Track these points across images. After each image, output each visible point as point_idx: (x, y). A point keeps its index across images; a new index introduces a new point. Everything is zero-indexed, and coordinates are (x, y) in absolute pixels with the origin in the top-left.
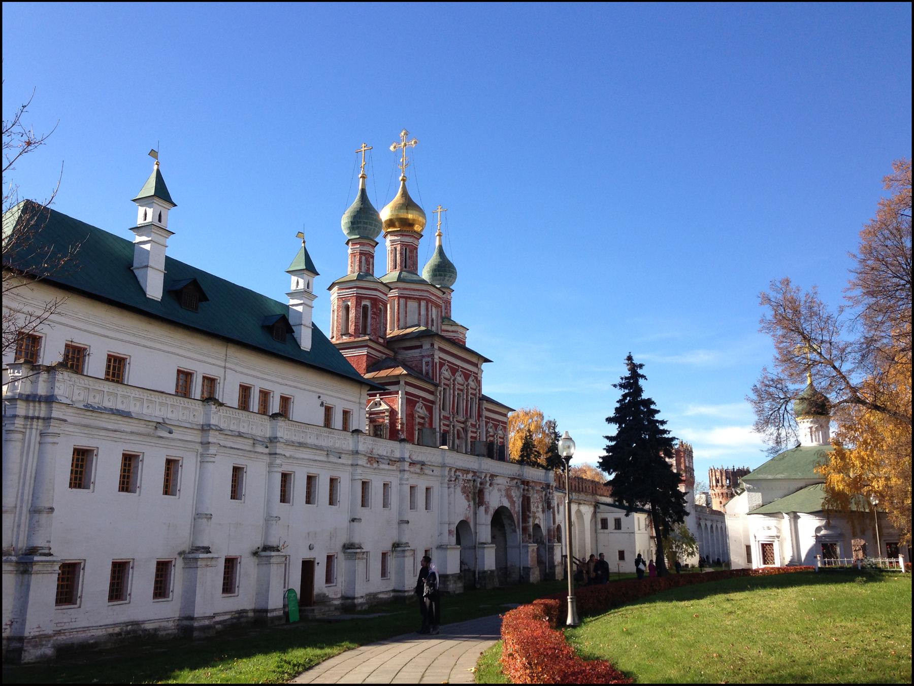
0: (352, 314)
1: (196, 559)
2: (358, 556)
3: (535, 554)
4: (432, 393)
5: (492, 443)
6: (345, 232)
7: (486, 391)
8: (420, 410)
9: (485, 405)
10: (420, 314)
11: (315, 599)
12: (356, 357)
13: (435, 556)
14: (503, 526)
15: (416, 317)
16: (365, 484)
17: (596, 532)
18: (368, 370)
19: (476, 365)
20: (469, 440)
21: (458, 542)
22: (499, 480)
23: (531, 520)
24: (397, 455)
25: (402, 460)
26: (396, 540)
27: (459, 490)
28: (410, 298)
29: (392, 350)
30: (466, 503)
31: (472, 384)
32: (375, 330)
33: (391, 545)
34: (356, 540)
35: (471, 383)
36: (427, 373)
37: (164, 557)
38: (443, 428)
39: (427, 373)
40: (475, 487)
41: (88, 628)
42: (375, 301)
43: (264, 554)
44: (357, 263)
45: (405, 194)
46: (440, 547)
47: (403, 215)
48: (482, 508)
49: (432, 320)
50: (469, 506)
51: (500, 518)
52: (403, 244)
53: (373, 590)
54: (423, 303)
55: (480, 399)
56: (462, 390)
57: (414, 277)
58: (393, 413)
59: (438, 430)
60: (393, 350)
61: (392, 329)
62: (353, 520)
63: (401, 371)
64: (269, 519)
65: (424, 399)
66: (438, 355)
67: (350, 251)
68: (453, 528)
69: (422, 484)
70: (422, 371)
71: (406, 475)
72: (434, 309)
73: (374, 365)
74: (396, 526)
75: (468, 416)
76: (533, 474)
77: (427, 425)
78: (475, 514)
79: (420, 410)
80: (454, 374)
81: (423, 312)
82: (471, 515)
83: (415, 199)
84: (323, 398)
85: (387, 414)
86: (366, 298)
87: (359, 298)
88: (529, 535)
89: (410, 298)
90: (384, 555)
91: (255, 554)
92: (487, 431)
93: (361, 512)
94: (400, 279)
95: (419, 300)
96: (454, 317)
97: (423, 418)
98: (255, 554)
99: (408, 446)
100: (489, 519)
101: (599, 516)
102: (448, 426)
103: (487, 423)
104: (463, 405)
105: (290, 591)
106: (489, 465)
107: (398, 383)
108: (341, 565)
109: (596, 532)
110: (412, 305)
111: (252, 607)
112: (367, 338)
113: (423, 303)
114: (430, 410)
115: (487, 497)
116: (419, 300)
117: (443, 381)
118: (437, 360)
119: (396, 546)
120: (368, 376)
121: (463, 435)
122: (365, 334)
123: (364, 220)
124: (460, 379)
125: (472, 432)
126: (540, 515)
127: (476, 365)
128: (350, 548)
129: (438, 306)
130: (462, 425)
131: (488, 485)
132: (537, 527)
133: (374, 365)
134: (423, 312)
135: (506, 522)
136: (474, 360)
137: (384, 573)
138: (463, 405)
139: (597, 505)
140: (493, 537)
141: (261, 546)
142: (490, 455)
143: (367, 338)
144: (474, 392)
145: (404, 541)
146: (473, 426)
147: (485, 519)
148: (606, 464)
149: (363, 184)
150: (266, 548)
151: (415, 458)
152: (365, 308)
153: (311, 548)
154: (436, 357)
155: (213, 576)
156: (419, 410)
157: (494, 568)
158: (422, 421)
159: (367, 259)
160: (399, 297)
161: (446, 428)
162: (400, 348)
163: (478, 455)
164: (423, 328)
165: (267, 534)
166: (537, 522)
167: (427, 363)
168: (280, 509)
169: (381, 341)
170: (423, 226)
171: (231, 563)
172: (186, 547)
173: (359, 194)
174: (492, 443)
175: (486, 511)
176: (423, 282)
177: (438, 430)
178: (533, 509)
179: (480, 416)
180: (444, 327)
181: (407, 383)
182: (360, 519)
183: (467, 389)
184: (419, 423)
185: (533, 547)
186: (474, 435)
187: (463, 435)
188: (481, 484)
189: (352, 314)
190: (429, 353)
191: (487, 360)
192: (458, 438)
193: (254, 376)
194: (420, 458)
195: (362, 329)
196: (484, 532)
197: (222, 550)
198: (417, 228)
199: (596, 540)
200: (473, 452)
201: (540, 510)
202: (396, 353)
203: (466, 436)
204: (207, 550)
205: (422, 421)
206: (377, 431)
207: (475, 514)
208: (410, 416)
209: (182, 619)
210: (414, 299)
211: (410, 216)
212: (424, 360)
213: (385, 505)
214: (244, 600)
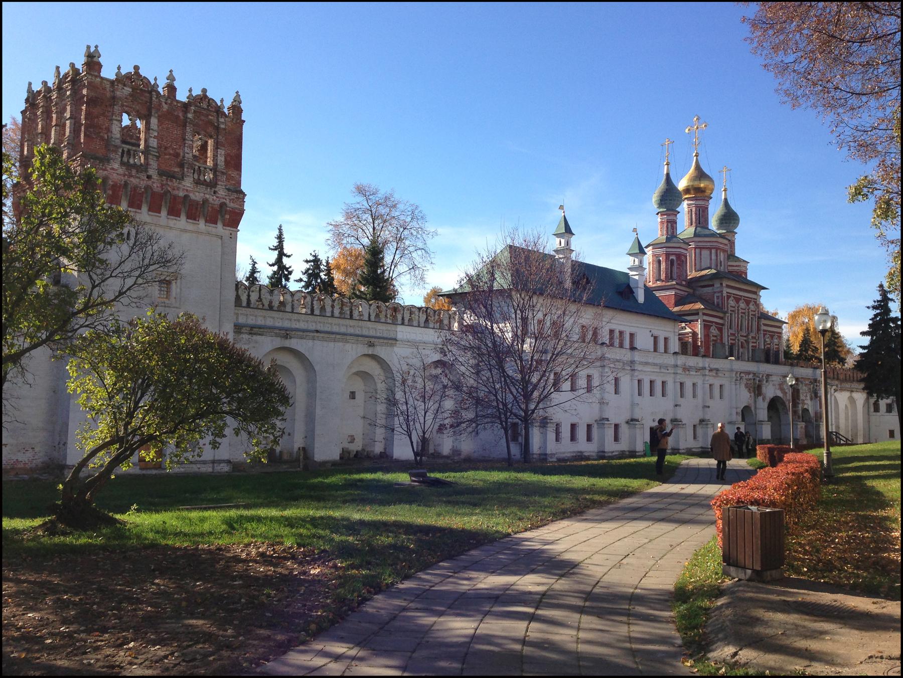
0: (663, 266)
4: (721, 318)
5: (769, 349)
6: (656, 206)
8: (714, 331)
9: (763, 321)
12: (667, 296)
14: (777, 410)
18: (676, 305)
19: (755, 293)
21: (743, 420)
22: (774, 378)
23: (800, 406)
24: (701, 365)
25: (704, 368)
26: (702, 417)
29: (692, 288)
30: (749, 395)
31: (752, 307)
32: (679, 276)
34: (678, 417)
36: (718, 305)
37: (590, 423)
39: (718, 305)
40: (755, 383)
41: (564, 453)
42: (679, 256)
44: (665, 229)
45: (698, 167)
47: (696, 183)
48: (760, 398)
51: (775, 405)
52: (697, 206)
53: (689, 446)
54: (713, 251)
55: (759, 318)
57: (707, 232)
58: (694, 334)
60: (692, 290)
61: (691, 271)
62: (676, 406)
63: (699, 306)
64: (633, 405)
65: (716, 323)
66: (726, 291)
67: (659, 220)
68: (740, 410)
69: (717, 383)
71: (707, 378)
73: (679, 301)
78: (755, 402)
79: (714, 331)
81: (714, 257)
82: (752, 402)
83: (706, 170)
87: (668, 255)
88: (799, 417)
90: (695, 426)
91: (627, 422)
92: (765, 341)
93: (681, 401)
94: (696, 235)
95: (710, 249)
96: (738, 254)
98: (627, 422)
99: (708, 360)
100: (766, 405)
103: (764, 335)
104: (745, 323)
105: (646, 442)
107: (697, 314)
110: (705, 253)
112: (674, 283)
113: (713, 251)
114: (720, 330)
115: (764, 390)
116: (710, 249)
117: (730, 309)
119: (702, 421)
120: (676, 309)
121: (745, 345)
122: (672, 279)
123: (669, 198)
124: (742, 305)
126: (808, 402)
127: (755, 293)
129: (724, 251)
133: (679, 301)
134: (714, 257)
135: (780, 407)
136: (754, 290)
137: (695, 438)
138: (745, 323)
142: (767, 361)
143: (674, 283)
145: (707, 418)
149: (668, 169)
150: (632, 420)
151: (712, 366)
152: (672, 261)
155: (610, 432)
159: (671, 225)
160: (695, 248)
164: (714, 271)
165: (632, 411)
166: (806, 407)
167: (718, 297)
168: (638, 399)
169: (684, 283)
170: (712, 190)
171: (616, 426)
172: (597, 418)
173: (665, 177)
174: (769, 349)
175: (764, 399)
176: (714, 235)
178: (802, 397)
179: (759, 330)
180: (730, 263)
181: (704, 314)
187: (745, 345)
189: (663, 266)
191: (764, 288)
192: (742, 347)
194: (715, 366)
195: (670, 277)
196: (762, 413)
197: (614, 420)
198: (708, 192)
200: (754, 359)
201: (808, 398)
202: (694, 290)
204: (607, 420)
206: (684, 345)
207: (755, 402)
208: (707, 336)
209: (599, 452)
211: (702, 185)
212: (716, 295)
213: (694, 396)
214: (623, 446)
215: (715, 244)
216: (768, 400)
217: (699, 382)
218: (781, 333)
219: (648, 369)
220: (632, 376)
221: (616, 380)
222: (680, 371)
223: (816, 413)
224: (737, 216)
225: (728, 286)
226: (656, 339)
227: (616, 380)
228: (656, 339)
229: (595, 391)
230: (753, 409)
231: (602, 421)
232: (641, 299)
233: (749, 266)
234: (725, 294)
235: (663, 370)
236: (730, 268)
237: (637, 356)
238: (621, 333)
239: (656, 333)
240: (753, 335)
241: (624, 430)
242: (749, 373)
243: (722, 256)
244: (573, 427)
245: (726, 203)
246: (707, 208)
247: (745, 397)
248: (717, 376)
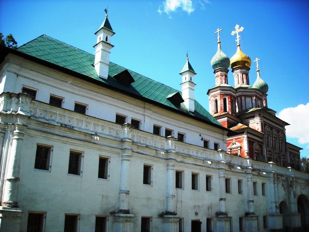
27: (280, 185)
35: (281, 135)
38: (268, 156)
50: (286, 194)
56: (276, 138)
59: (266, 156)
69: (259, 181)
72: (259, 101)
73: (231, 124)
77: (260, 154)
84: (202, 136)
102: (270, 155)
104: (277, 145)
114: (261, 146)
117: (267, 133)
124: (275, 132)
130: (278, 155)
138: (277, 145)
144: (282, 139)
158: (257, 152)
161: (270, 156)
177: (266, 156)
183: (279, 137)
184: (256, 153)
187: (278, 160)
188: (291, 182)
193: (161, 121)
203: (280, 161)
205: (257, 152)
247: (282, 193)
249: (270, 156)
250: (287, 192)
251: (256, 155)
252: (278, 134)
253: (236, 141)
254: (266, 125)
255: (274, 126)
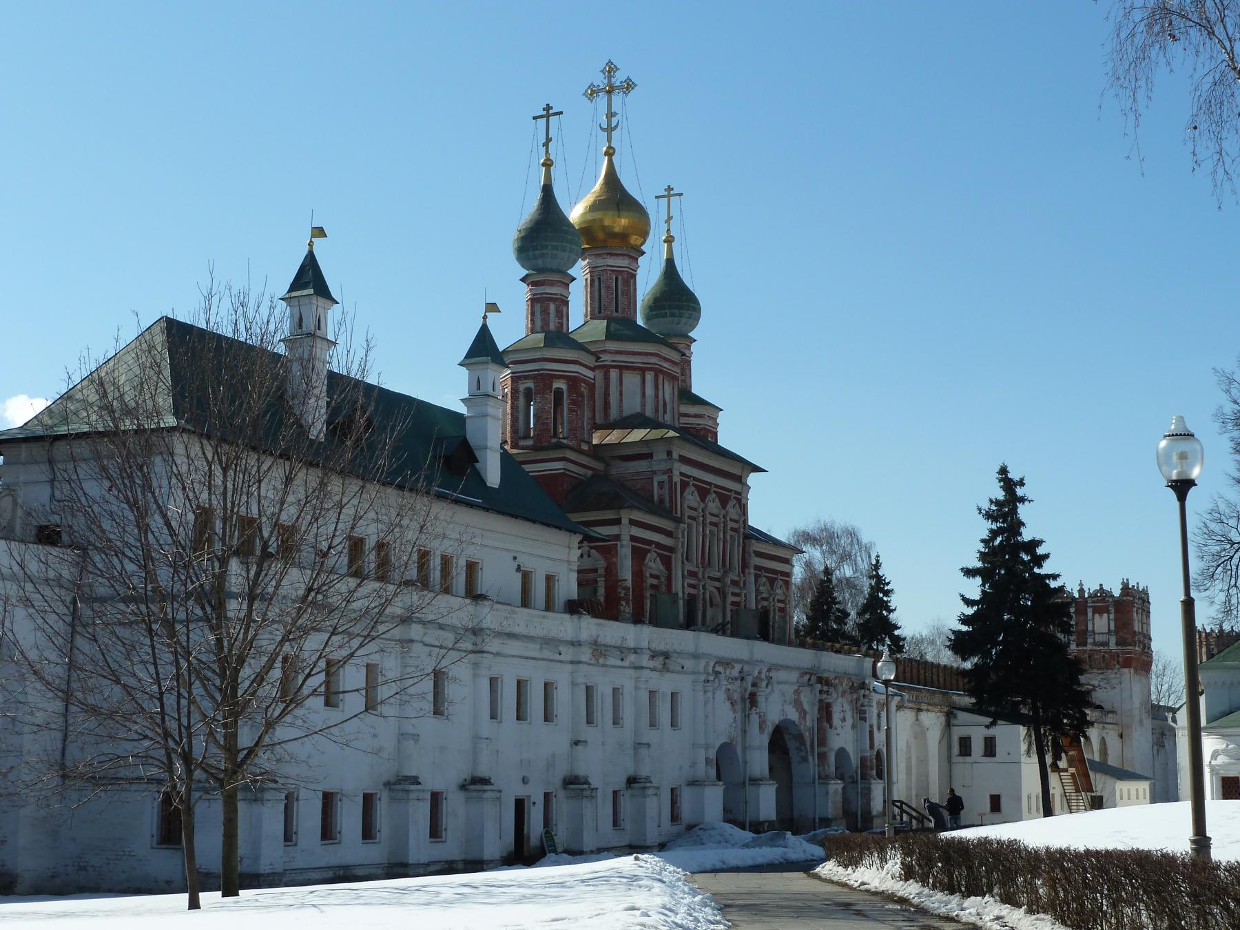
1: (408, 791)
2: (585, 793)
3: (839, 798)
4: (669, 534)
7: (756, 520)
8: (653, 564)
10: (644, 395)
11: (526, 854)
13: (687, 796)
14: (785, 751)
15: (638, 398)
16: (589, 690)
17: (950, 762)
20: (729, 608)
21: (719, 778)
26: (631, 772)
27: (721, 695)
28: (627, 368)
30: (732, 715)
33: (624, 780)
34: (581, 771)
36: (661, 501)
39: (661, 501)
43: (472, 787)
46: (693, 783)
49: (665, 404)
51: (781, 741)
54: (649, 377)
56: (715, 524)
59: (680, 595)
62: (576, 743)
65: (658, 545)
68: (712, 754)
69: (665, 684)
70: (652, 496)
74: (631, 752)
75: (726, 568)
76: (836, 662)
77: (663, 589)
78: (744, 732)
79: (653, 564)
80: (703, 499)
81: (649, 391)
85: (601, 571)
86: (560, 377)
89: (627, 368)
90: (615, 793)
91: (463, 787)
93: (588, 733)
95: (642, 371)
97: (657, 577)
100: (765, 739)
101: (957, 732)
103: (757, 577)
104: (717, 550)
106: (764, 651)
108: (563, 807)
109: (950, 762)
111: (462, 857)
113: (649, 377)
114: (667, 562)
116: (642, 371)
117: (688, 512)
118: (677, 479)
119: (632, 781)
124: (713, 505)
125: (734, 594)
128: (574, 783)
129: (673, 378)
130: (717, 584)
131: (764, 684)
132: (842, 753)
134: (649, 391)
135: (792, 745)
136: (735, 470)
137: (616, 823)
139: (950, 715)
140: (771, 769)
141: (469, 779)
146: (735, 583)
147: (761, 739)
148: (960, 644)
151: (654, 646)
153: (525, 781)
154: (676, 473)
156: (652, 564)
157: (773, 817)
158: (655, 582)
161: (692, 591)
162: (614, 458)
163: (747, 638)
167: (661, 483)
171: (436, 798)
177: (680, 595)
179: (745, 565)
182: (586, 742)
184: (652, 586)
185: (836, 786)
186: (735, 599)
190: (663, 466)
194: (662, 647)
199: (948, 774)
205: (655, 582)
207: (744, 732)
208: (638, 575)
210: (634, 369)
212: (656, 479)
213: (616, 721)
215: (653, 360)
216: (769, 729)
217: (628, 687)
218: (788, 575)
219: (514, 647)
220: (476, 665)
221: (439, 676)
222: (585, 655)
223: (863, 760)
224: (696, 301)
225: (683, 460)
226: (526, 577)
227: (439, 676)
228: (526, 577)
229: (385, 709)
230: (739, 750)
231: (402, 784)
232: (493, 476)
233: (721, 418)
234: (677, 478)
235: (547, 654)
236: (683, 420)
237: (489, 617)
238: (446, 562)
239: (528, 563)
240: (733, 576)
241: (455, 806)
242: (727, 663)
243: (668, 391)
244: (328, 800)
245: (670, 269)
246: (634, 276)
247: (722, 720)
248: (665, 668)
249: (692, 591)
250: (739, 715)
251: (653, 592)
252: (723, 512)
253: (591, 548)
254: (688, 483)
255: (710, 484)
